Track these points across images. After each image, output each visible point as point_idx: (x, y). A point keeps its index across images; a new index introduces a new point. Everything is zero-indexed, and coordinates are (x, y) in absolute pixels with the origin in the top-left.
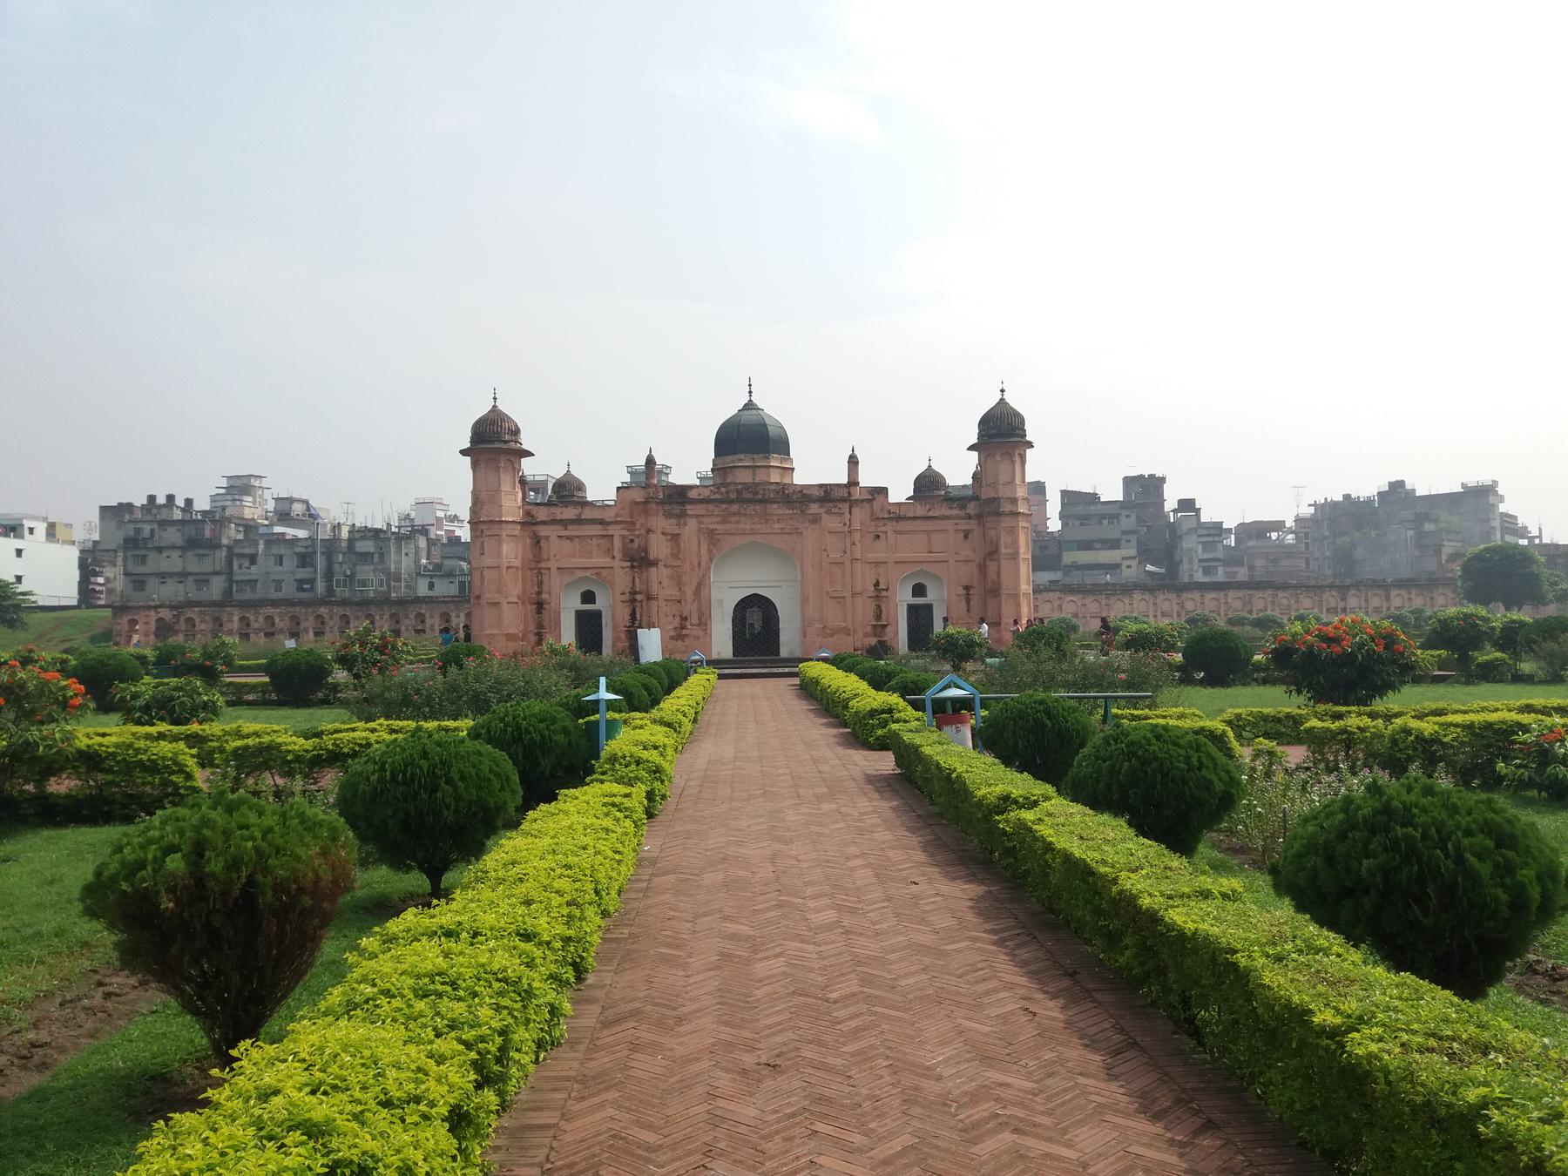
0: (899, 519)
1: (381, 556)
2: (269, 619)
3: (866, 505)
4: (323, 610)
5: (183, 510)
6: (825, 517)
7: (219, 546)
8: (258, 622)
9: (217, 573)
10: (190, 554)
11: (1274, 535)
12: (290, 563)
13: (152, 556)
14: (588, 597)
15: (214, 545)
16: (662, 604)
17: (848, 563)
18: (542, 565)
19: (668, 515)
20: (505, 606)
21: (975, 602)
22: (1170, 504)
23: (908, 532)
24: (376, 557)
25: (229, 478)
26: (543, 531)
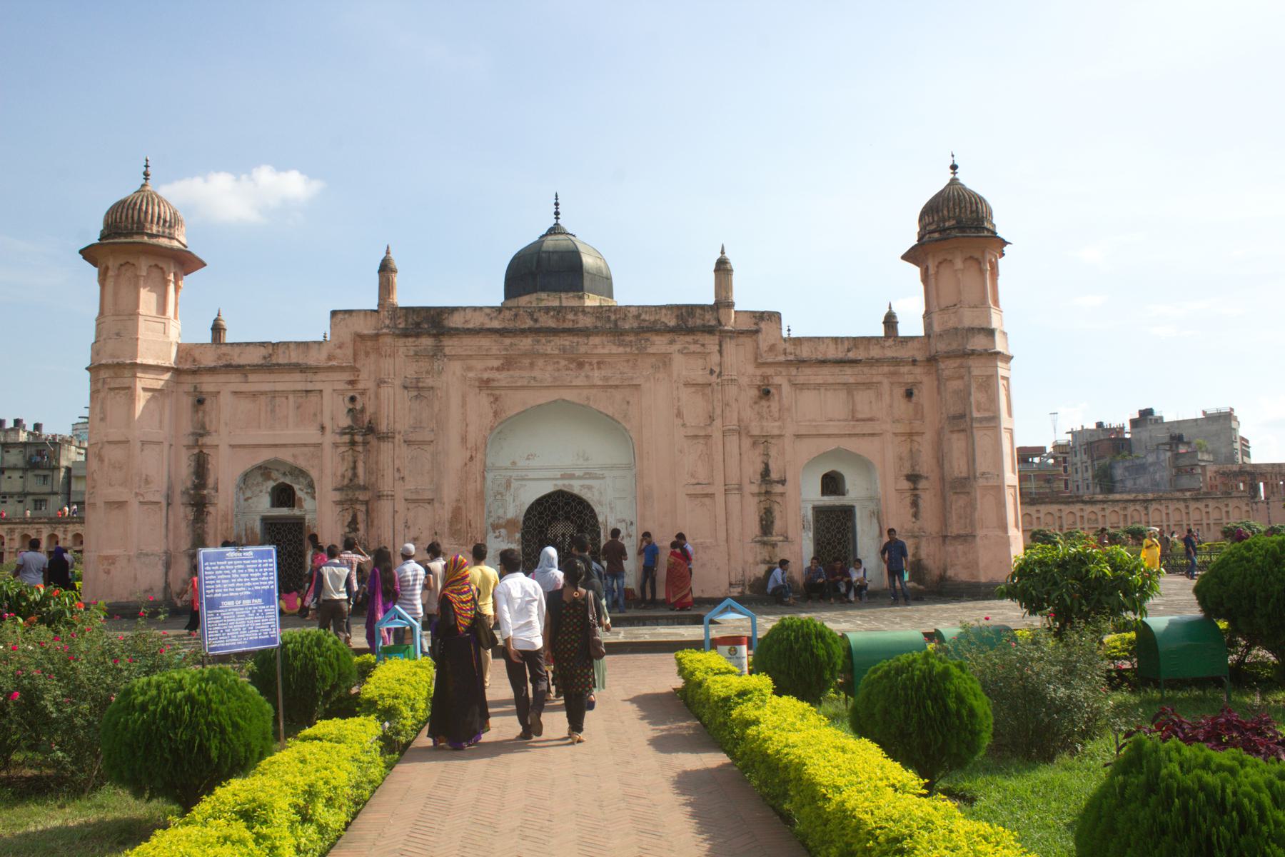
0: (801, 362)
3: (748, 342)
5: (30, 433)
6: (678, 360)
9: (56, 494)
10: (30, 474)
11: (1037, 460)
14: (284, 496)
16: (401, 506)
17: (717, 435)
18: (207, 440)
20: (134, 506)
21: (928, 500)
23: (817, 387)
26: (208, 384)
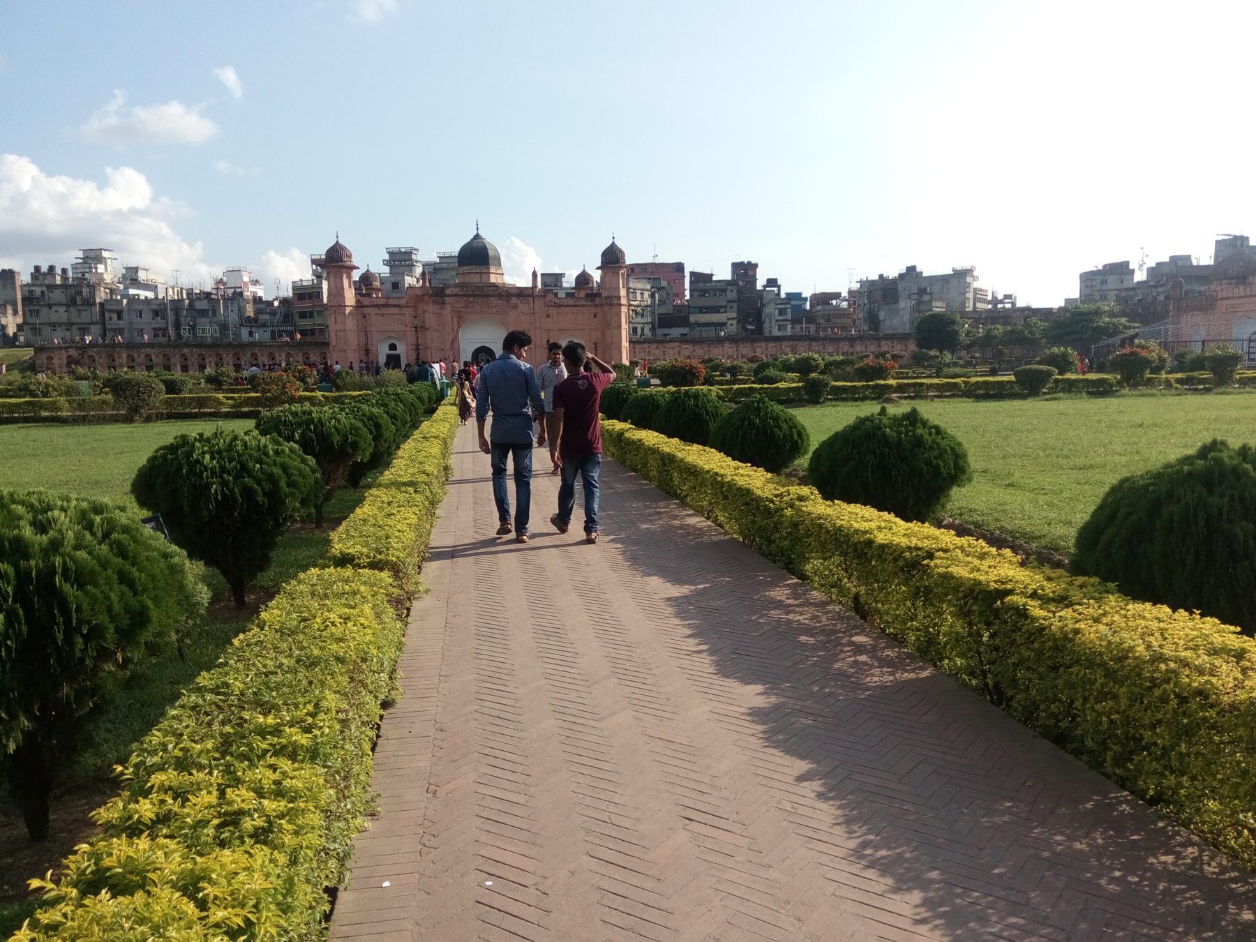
1: (215, 312)
2: (148, 356)
4: (186, 351)
7: (94, 304)
8: (140, 358)
9: (96, 323)
10: (72, 309)
12: (147, 317)
13: (45, 310)
14: (393, 347)
15: (89, 303)
19: (435, 302)
20: (349, 352)
22: (760, 283)
24: (210, 313)
25: (84, 251)
26: (367, 311)
